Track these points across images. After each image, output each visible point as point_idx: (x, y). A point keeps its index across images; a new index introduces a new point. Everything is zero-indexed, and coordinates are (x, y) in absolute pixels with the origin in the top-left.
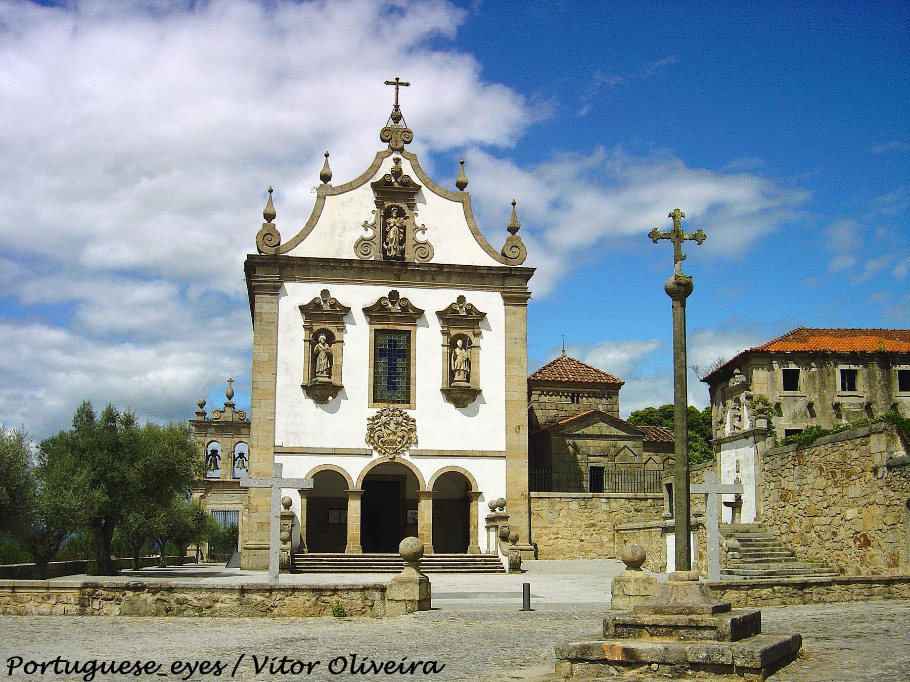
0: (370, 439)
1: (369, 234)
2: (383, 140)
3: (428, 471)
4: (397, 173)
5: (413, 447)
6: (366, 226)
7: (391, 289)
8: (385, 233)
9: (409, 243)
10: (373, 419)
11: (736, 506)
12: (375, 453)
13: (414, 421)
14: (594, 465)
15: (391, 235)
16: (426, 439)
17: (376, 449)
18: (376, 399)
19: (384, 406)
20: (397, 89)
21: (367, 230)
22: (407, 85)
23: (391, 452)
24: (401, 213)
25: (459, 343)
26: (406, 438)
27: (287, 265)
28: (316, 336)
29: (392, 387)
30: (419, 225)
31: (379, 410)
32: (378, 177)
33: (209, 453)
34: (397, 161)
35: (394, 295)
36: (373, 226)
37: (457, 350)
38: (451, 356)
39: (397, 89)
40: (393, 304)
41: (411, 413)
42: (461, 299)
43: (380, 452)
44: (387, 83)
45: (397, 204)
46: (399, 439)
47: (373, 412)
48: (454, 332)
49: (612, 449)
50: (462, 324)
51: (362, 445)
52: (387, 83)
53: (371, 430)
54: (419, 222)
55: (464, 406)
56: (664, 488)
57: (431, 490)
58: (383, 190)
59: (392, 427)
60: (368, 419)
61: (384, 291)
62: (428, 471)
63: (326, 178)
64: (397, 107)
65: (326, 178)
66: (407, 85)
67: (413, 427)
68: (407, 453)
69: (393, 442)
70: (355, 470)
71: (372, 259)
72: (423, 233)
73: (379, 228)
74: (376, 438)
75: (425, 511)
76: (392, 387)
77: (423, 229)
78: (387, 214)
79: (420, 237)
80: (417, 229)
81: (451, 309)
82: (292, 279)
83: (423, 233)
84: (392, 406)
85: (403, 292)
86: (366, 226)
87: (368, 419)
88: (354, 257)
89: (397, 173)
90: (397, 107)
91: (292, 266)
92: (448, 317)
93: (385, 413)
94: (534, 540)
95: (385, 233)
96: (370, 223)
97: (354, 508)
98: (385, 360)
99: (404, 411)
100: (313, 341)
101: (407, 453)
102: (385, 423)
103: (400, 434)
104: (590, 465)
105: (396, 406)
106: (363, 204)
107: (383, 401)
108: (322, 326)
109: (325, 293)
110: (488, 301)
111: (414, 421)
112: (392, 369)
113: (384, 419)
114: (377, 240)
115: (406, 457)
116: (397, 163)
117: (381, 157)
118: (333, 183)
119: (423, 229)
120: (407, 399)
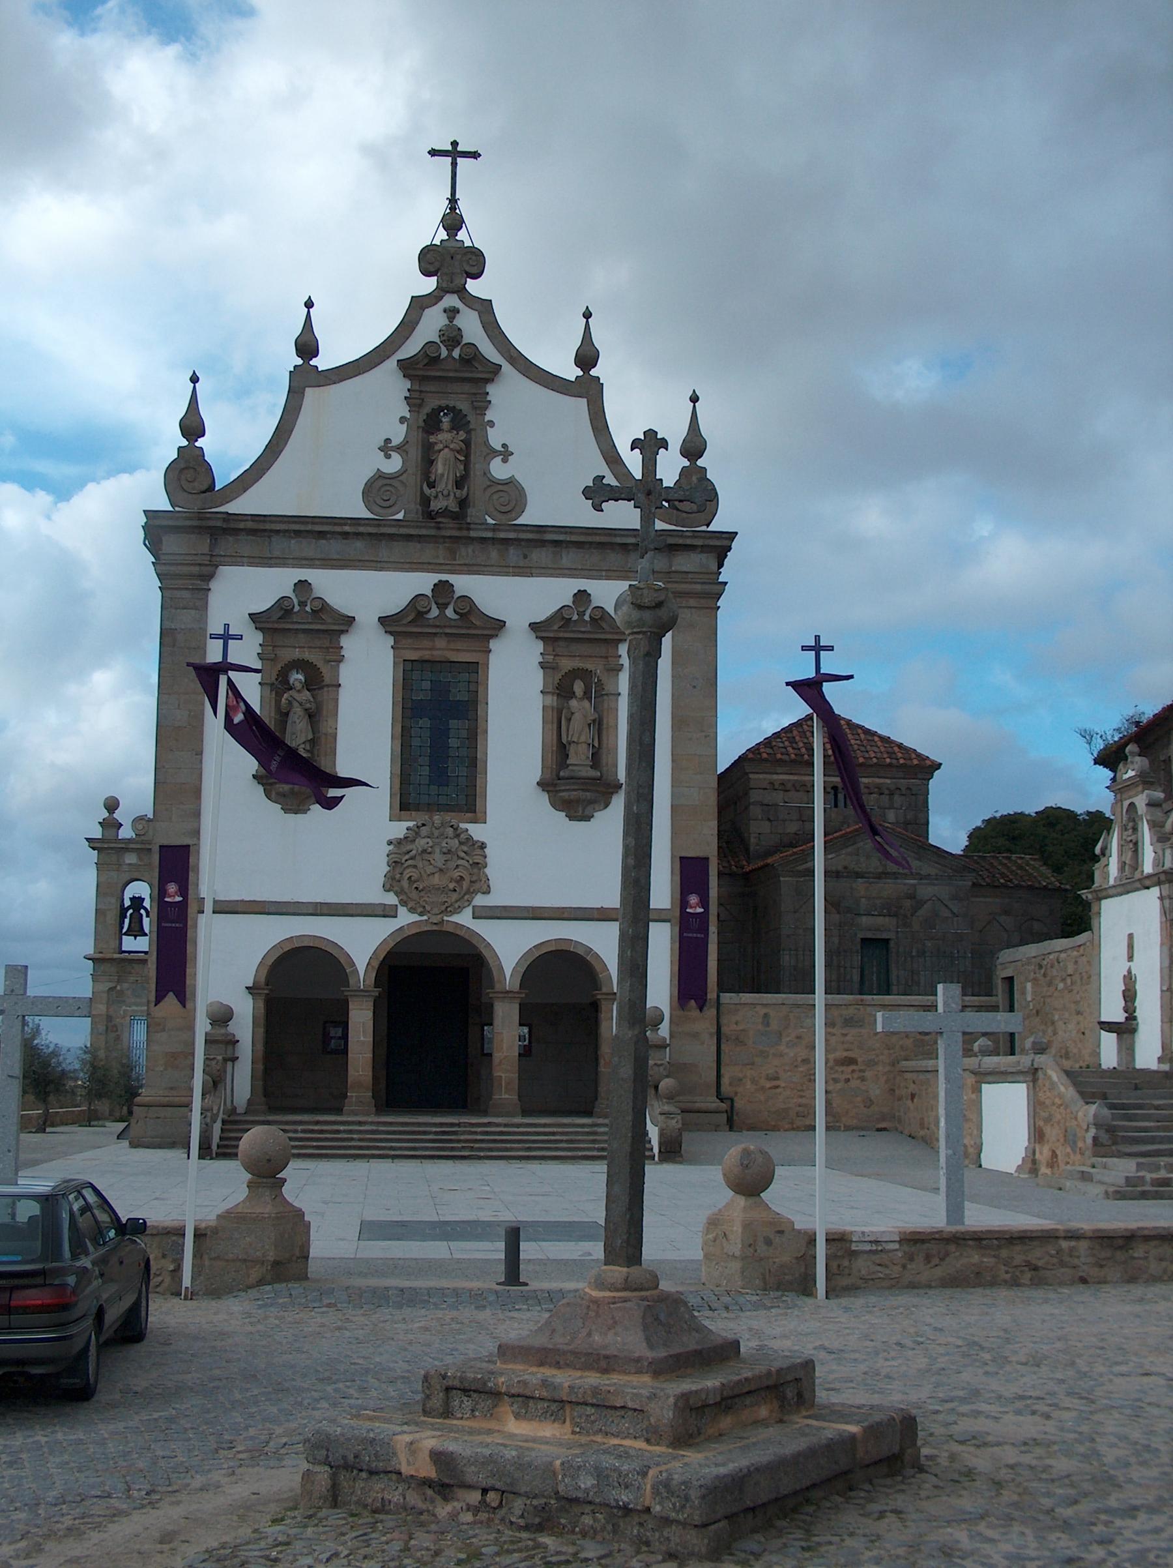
0: (391, 883)
1: (394, 464)
2: (427, 273)
3: (509, 947)
4: (452, 337)
5: (480, 900)
6: (386, 448)
7: (435, 578)
8: (428, 462)
9: (476, 483)
10: (399, 843)
11: (1126, 1029)
12: (402, 911)
13: (483, 846)
15: (440, 467)
16: (507, 882)
17: (403, 903)
18: (405, 802)
19: (423, 817)
20: (454, 165)
21: (388, 457)
22: (475, 155)
23: (436, 911)
24: (460, 422)
25: (578, 687)
26: (465, 884)
27: (226, 531)
28: (283, 675)
29: (440, 776)
31: (411, 824)
32: (411, 349)
33: (127, 903)
34: (452, 313)
35: (442, 588)
36: (399, 449)
37: (574, 703)
39: (454, 165)
40: (442, 607)
41: (476, 831)
42: (582, 596)
43: (412, 910)
44: (434, 153)
45: (451, 404)
46: (451, 886)
47: (400, 829)
48: (567, 664)
49: (908, 903)
51: (376, 895)
52: (434, 153)
53: (394, 864)
54: (495, 438)
55: (587, 818)
56: (1000, 987)
57: (516, 987)
58: (424, 372)
59: (438, 859)
60: (390, 843)
61: (422, 582)
62: (509, 947)
63: (307, 347)
64: (453, 201)
65: (307, 347)
66: (475, 155)
67: (478, 859)
68: (468, 912)
69: (443, 890)
70: (361, 944)
71: (400, 516)
72: (505, 461)
73: (415, 453)
74: (405, 883)
75: (506, 1033)
76: (440, 776)
77: (506, 454)
78: (431, 424)
79: (499, 470)
80: (494, 453)
81: (561, 617)
82: (237, 560)
83: (505, 461)
84: (437, 818)
85: (464, 584)
86: (386, 448)
87: (390, 843)
88: (363, 513)
89: (452, 337)
90: (453, 201)
91: (236, 531)
92: (554, 632)
93: (424, 831)
94: (726, 1089)
95: (428, 462)
96: (396, 442)
97: (361, 1020)
98: (425, 722)
99: (463, 826)
101: (468, 912)
102: (424, 851)
103: (456, 874)
104: (861, 935)
105: (448, 817)
106: (385, 406)
107: (417, 808)
108: (296, 654)
109: (302, 586)
111: (483, 846)
112: (439, 738)
113: (421, 843)
115: (464, 918)
116: (451, 319)
117: (418, 305)
118: (322, 362)
120: (470, 802)
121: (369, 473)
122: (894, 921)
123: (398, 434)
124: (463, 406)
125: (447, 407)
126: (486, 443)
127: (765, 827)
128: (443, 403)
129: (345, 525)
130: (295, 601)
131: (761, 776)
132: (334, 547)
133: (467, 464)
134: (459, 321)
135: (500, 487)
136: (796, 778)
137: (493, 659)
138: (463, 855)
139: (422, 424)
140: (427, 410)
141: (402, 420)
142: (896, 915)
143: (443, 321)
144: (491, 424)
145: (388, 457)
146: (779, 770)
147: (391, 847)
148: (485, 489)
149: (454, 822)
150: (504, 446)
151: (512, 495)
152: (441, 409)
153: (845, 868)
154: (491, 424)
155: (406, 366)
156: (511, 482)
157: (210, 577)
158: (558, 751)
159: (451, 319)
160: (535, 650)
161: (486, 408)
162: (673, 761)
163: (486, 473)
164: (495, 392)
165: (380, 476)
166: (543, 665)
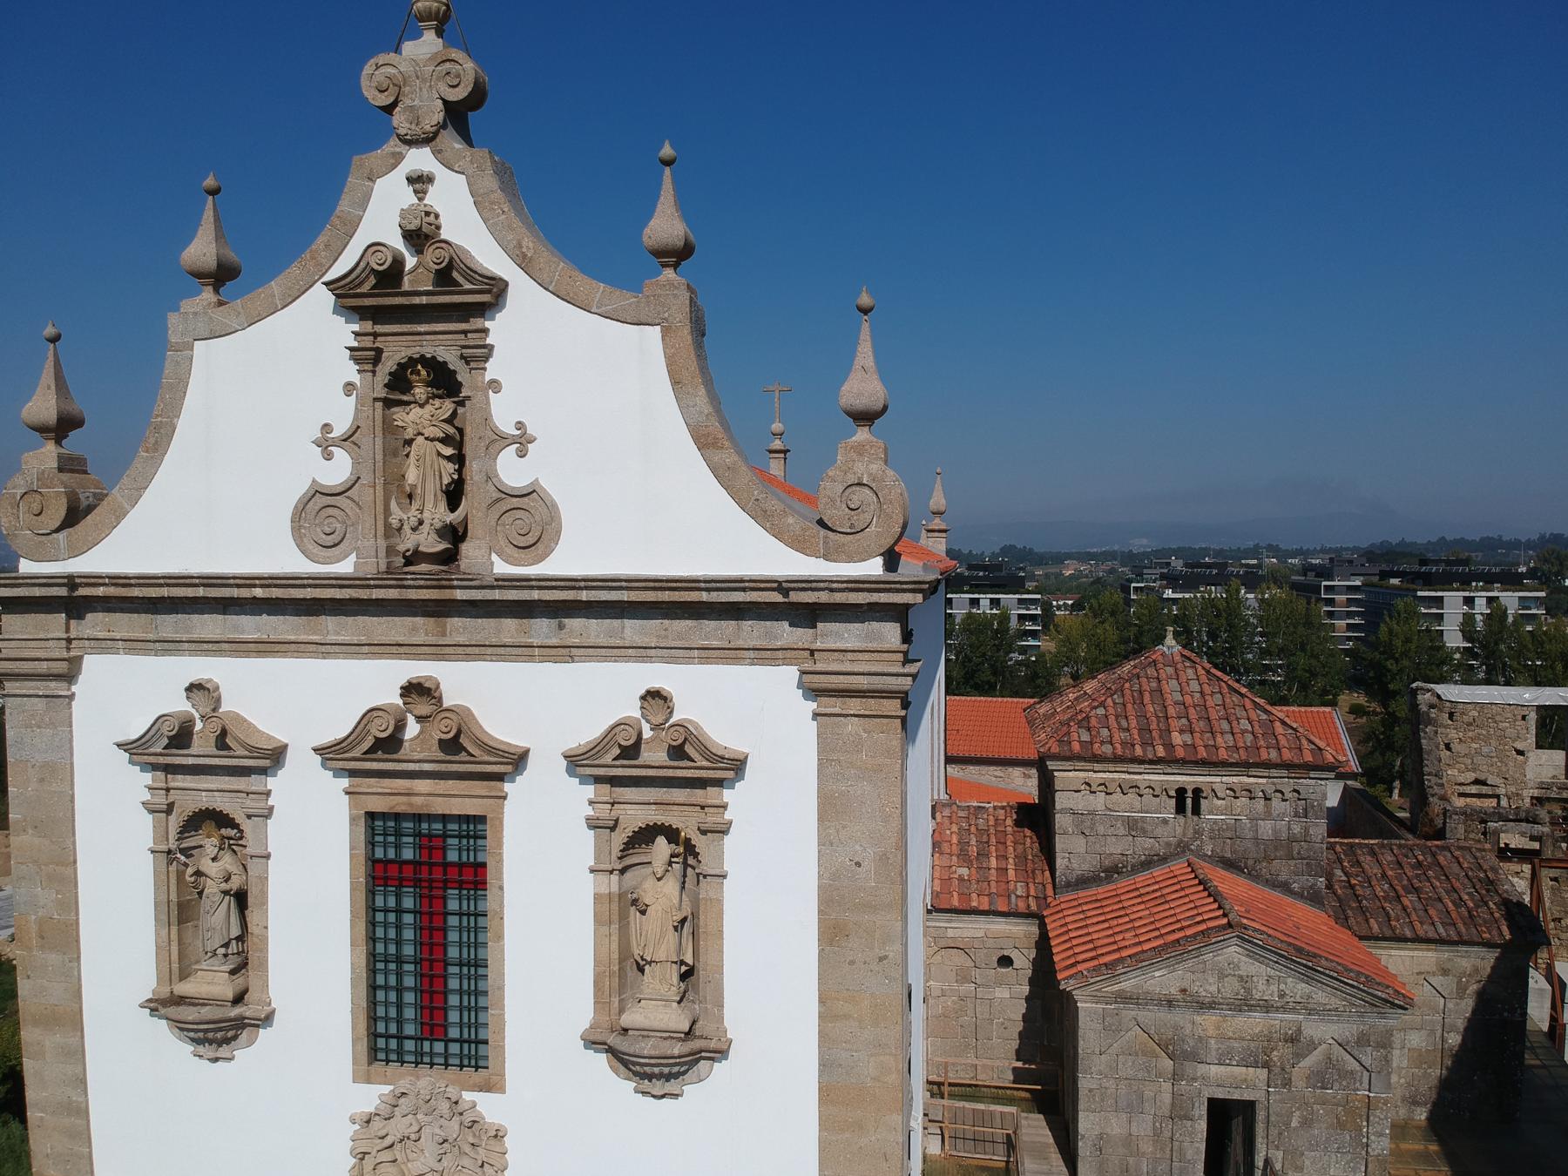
1: (338, 469)
13: (498, 1136)
14: (1220, 1094)
21: (328, 457)
24: (445, 382)
30: (506, 425)
35: (415, 690)
36: (347, 439)
38: (621, 909)
41: (487, 1106)
45: (429, 351)
50: (660, 792)
54: (503, 412)
72: (522, 454)
73: (373, 444)
79: (511, 471)
80: (502, 440)
82: (105, 645)
83: (522, 454)
86: (325, 444)
96: (339, 430)
99: (468, 1096)
100: (175, 857)
104: (1209, 1092)
108: (205, 801)
110: (752, 706)
114: (363, 493)
119: (523, 441)
121: (301, 489)
122: (1262, 1074)
123: (343, 413)
124: (448, 355)
125: (423, 360)
126: (487, 420)
127: (1079, 844)
128: (415, 352)
129: (255, 586)
130: (197, 716)
131: (1071, 774)
132: (250, 626)
133: (459, 459)
134: (433, 198)
135: (515, 502)
136: (1123, 776)
137: (509, 807)
138: (467, 1149)
139: (381, 392)
140: (388, 365)
141: (349, 388)
142: (1266, 1065)
143: (408, 197)
144: (495, 385)
145: (328, 457)
146: (1097, 766)
147: (357, 1127)
148: (490, 506)
149: (452, 1091)
150: (520, 425)
151: (533, 518)
152: (412, 362)
153: (1184, 991)
154: (495, 385)
155: (347, 295)
156: (531, 492)
157: (70, 677)
158: (622, 971)
159: (420, 194)
160: (580, 797)
161: (486, 358)
162: (822, 1001)
163: (490, 476)
164: (499, 328)
165: (317, 491)
166: (593, 824)
